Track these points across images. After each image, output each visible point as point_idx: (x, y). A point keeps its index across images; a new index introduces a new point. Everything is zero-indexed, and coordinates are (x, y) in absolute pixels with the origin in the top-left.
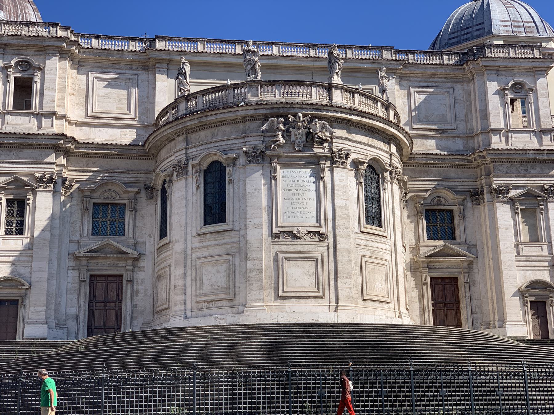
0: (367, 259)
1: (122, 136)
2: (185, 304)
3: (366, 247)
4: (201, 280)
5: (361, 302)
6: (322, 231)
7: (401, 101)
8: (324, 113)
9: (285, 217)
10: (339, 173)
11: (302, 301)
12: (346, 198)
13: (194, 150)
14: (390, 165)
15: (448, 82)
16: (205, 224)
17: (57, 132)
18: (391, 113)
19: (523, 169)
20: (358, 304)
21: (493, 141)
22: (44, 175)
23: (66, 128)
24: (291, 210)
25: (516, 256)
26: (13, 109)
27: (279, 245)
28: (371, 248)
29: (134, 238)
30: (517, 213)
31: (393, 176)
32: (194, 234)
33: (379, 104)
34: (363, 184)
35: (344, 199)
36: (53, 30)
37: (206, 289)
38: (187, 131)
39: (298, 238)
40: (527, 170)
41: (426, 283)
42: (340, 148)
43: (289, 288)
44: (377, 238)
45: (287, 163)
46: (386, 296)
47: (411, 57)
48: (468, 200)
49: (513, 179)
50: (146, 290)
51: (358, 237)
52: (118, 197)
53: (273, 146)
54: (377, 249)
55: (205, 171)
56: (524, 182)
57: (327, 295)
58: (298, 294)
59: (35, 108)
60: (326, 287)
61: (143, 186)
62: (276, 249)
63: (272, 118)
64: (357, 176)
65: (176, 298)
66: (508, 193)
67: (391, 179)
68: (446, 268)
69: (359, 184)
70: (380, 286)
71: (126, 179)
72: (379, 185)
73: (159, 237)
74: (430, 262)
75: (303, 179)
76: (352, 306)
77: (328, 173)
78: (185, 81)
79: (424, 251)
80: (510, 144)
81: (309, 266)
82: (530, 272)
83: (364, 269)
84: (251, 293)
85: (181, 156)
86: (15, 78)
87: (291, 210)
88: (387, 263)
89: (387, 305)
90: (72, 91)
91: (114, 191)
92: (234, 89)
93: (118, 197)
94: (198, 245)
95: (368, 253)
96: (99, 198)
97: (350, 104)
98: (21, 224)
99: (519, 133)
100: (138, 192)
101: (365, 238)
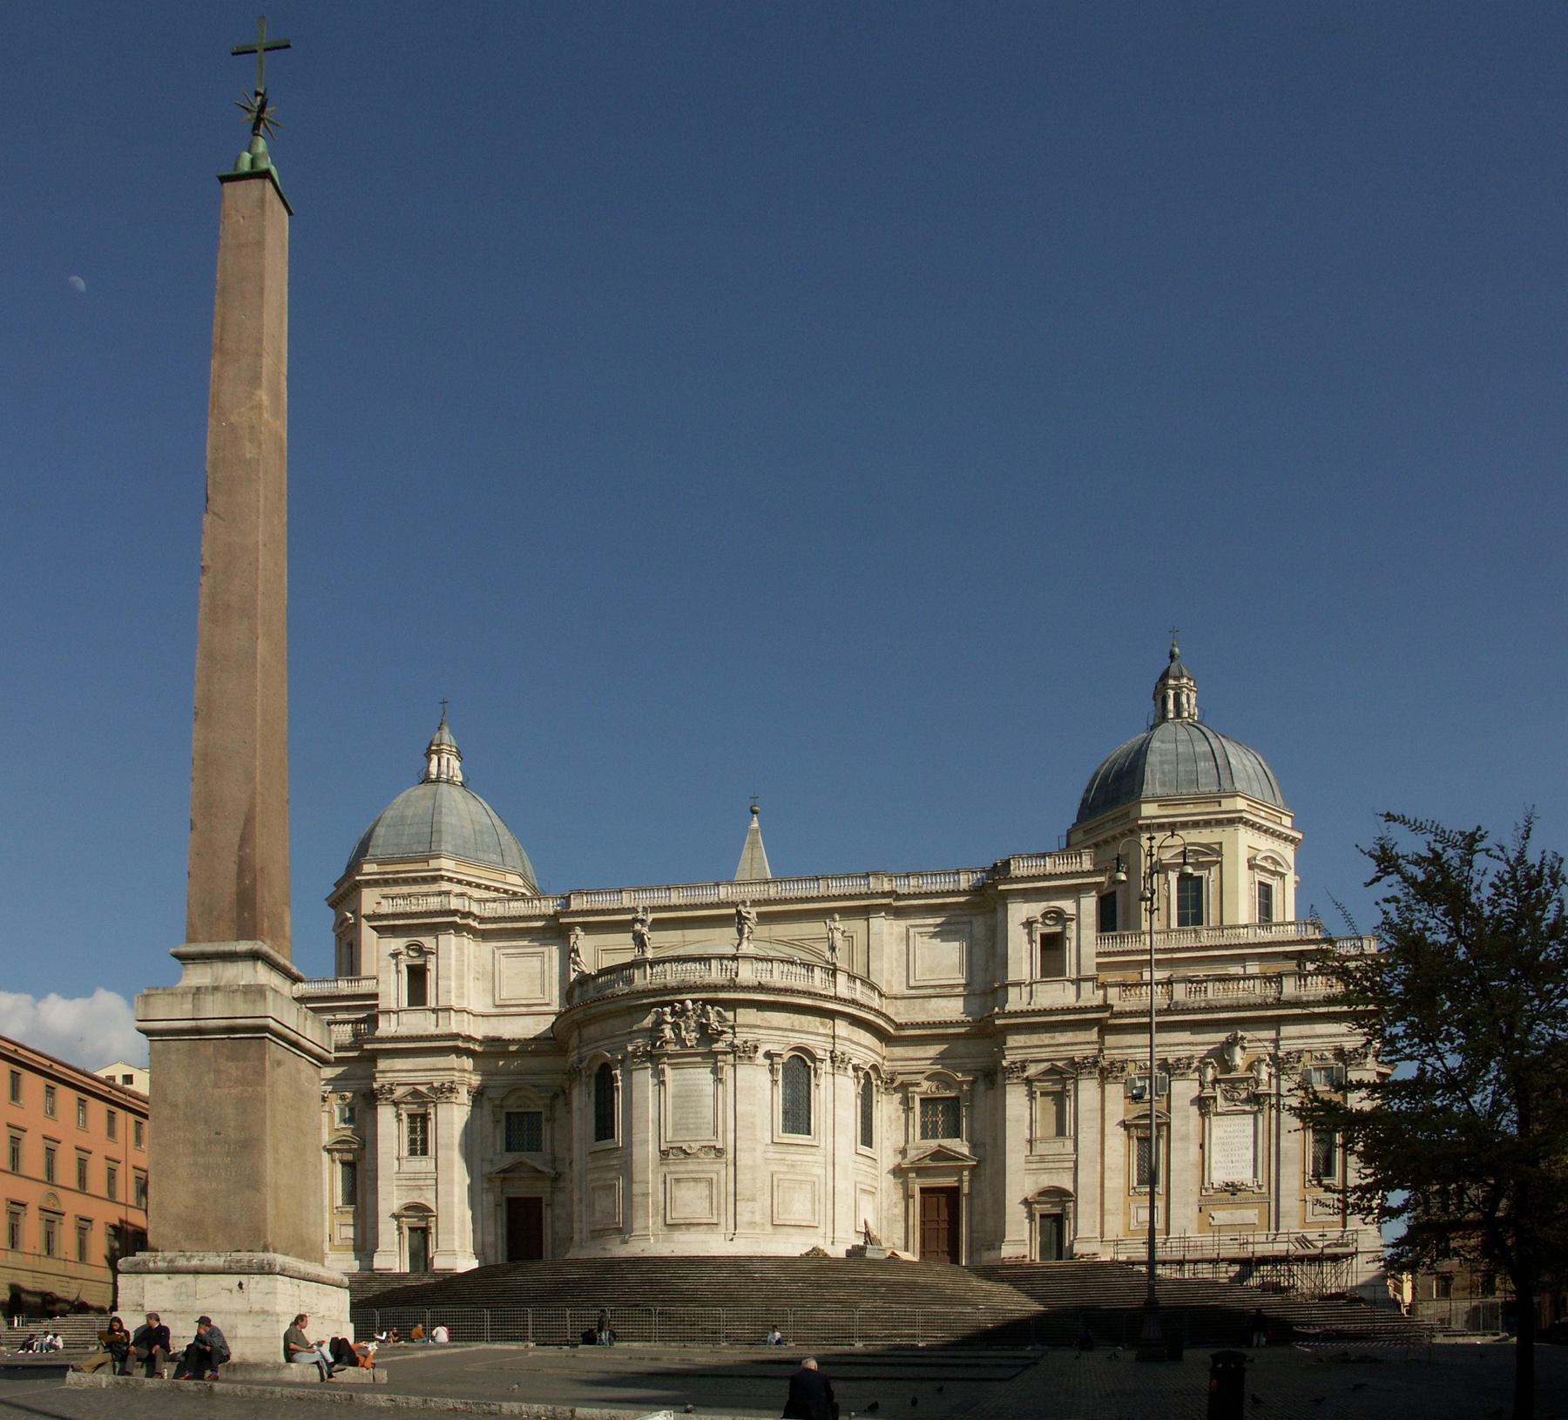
0: (781, 1176)
4: (594, 1204)
5: (769, 1228)
6: (719, 1146)
9: (675, 1130)
10: (744, 1071)
11: (693, 1229)
13: (585, 1049)
14: (832, 1052)
20: (764, 1230)
21: (1009, 999)
22: (443, 1084)
23: (469, 1023)
24: (684, 1121)
26: (409, 1005)
27: (667, 1165)
30: (1035, 1098)
31: (837, 1065)
34: (780, 1083)
37: (598, 1215)
38: (579, 1025)
39: (689, 1154)
42: (744, 1039)
43: (677, 1215)
44: (801, 1149)
45: (678, 1064)
53: (658, 1044)
56: (1047, 1054)
57: (723, 1220)
58: (688, 1221)
60: (723, 1212)
61: (560, 1089)
62: (665, 1168)
66: (1024, 1071)
67: (834, 1069)
69: (774, 1082)
72: (809, 1081)
74: (919, 1168)
75: (698, 1082)
77: (728, 1072)
80: (1032, 1003)
81: (702, 1189)
83: (775, 1188)
84: (638, 1221)
87: (684, 1121)
88: (815, 1179)
89: (812, 1229)
93: (532, 1106)
94: (590, 1165)
95: (784, 1169)
97: (765, 979)
100: (555, 1097)
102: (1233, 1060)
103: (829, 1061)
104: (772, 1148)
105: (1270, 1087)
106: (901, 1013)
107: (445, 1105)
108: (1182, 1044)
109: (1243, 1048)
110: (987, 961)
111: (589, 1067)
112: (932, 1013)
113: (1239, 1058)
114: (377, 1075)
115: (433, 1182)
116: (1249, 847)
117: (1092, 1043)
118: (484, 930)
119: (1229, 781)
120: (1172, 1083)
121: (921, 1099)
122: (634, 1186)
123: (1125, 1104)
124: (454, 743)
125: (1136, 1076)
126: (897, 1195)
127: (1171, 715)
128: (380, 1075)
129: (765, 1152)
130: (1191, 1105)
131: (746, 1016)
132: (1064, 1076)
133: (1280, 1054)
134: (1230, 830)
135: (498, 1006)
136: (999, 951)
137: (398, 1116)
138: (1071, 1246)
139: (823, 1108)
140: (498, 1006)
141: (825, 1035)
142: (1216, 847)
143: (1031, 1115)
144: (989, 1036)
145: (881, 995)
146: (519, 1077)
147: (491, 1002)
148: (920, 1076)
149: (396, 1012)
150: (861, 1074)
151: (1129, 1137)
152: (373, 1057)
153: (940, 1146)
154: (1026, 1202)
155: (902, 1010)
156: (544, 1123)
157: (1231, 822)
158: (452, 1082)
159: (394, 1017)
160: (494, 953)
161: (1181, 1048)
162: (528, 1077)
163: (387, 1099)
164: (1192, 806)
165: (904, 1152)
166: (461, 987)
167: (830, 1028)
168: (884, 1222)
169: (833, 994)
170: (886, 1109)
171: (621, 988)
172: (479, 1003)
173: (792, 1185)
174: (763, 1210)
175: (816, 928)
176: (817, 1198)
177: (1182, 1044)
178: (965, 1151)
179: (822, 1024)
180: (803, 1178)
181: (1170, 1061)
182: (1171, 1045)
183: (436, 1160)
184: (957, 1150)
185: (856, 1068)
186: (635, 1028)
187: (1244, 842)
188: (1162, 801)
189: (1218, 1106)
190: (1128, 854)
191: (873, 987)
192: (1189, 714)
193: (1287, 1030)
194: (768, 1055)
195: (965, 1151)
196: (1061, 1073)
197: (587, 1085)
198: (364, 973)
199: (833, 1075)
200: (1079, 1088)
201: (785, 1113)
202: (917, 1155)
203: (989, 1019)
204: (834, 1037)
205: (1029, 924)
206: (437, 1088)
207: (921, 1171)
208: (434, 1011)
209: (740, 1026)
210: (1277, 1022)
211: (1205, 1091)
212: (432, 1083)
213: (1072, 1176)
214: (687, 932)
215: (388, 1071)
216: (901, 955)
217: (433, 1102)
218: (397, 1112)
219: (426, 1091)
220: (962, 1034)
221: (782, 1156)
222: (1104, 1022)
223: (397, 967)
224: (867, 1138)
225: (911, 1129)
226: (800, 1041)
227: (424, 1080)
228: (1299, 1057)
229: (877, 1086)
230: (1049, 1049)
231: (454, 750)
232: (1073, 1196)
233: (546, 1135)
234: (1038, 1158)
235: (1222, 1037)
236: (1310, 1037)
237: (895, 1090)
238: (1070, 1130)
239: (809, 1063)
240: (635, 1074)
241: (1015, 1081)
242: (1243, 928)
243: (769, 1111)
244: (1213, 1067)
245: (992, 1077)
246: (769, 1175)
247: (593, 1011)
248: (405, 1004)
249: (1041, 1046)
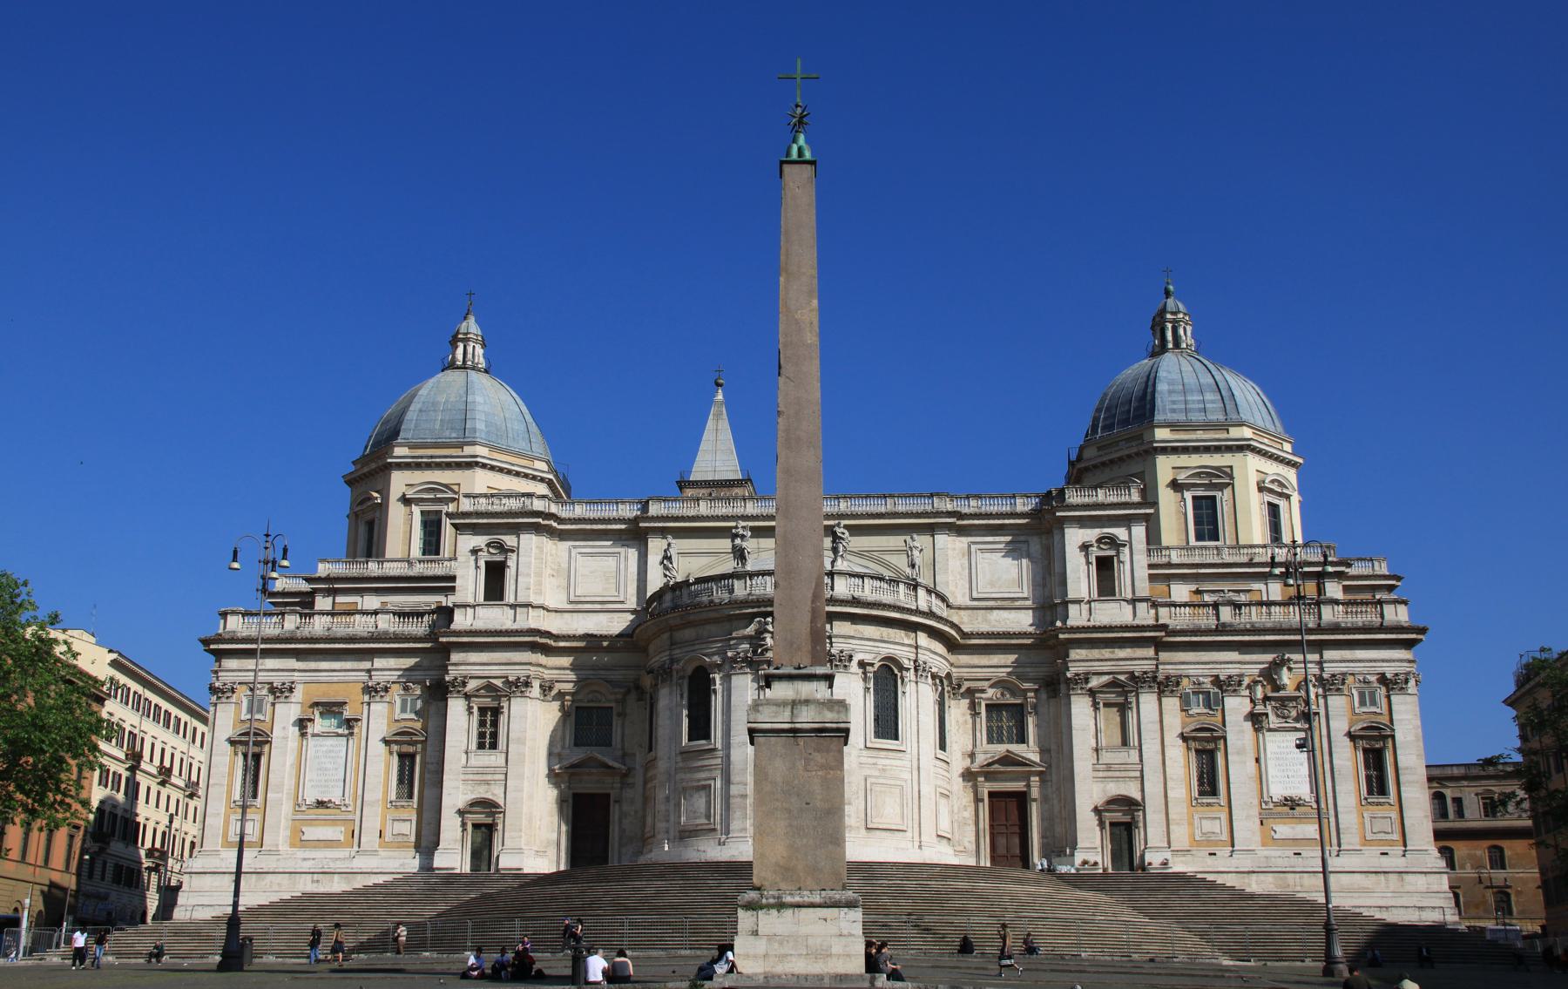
0: (873, 780)
1: (610, 624)
2: (667, 832)
5: (863, 831)
7: (958, 563)
13: (677, 651)
14: (915, 661)
15: (1022, 535)
16: (689, 740)
17: (532, 627)
18: (921, 592)
23: (544, 618)
28: (881, 767)
29: (623, 749)
30: (1098, 709)
31: (920, 673)
32: (678, 752)
33: (902, 586)
34: (872, 690)
36: (528, 501)
41: (982, 800)
44: (890, 753)
46: (901, 823)
47: (973, 503)
48: (1042, 689)
50: (636, 812)
52: (604, 700)
53: (759, 651)
55: (691, 678)
56: (1109, 668)
59: (509, 597)
63: (758, 619)
64: (865, 679)
65: (661, 825)
66: (1087, 682)
70: (892, 811)
71: (612, 677)
73: (647, 750)
74: (988, 772)
78: (670, 566)
79: (981, 759)
80: (1092, 620)
83: (868, 792)
84: (735, 822)
85: (664, 657)
86: (487, 563)
88: (903, 783)
89: (901, 833)
90: (552, 572)
91: (601, 693)
92: (721, 580)
94: (681, 765)
95: (877, 773)
96: (581, 701)
97: (857, 594)
98: (494, 735)
100: (628, 692)
102: (1280, 678)
103: (912, 671)
104: (865, 753)
105: (1318, 707)
106: (969, 622)
107: (519, 699)
108: (1231, 663)
109: (1290, 669)
110: (1044, 578)
111: (683, 669)
112: (996, 624)
113: (1286, 678)
114: (449, 668)
115: (503, 777)
116: (1258, 471)
117: (1150, 659)
118: (562, 530)
119: (1235, 411)
120: (1225, 699)
121: (987, 705)
122: (731, 786)
123: (1182, 718)
124: (480, 333)
125: (1190, 691)
126: (968, 797)
127: (1170, 345)
128: (453, 668)
129: (859, 756)
130: (1245, 721)
131: (841, 628)
132: (1126, 689)
133: (1325, 676)
134: (1239, 455)
135: (571, 602)
136: (1057, 569)
137: (470, 709)
138: (1142, 856)
139: (908, 716)
140: (571, 602)
142: (1228, 470)
143: (1096, 725)
144: (1051, 648)
145: (948, 606)
146: (592, 672)
147: (565, 599)
148: (986, 684)
149: (474, 607)
150: (938, 681)
151: (1188, 749)
152: (447, 649)
153: (1008, 751)
154: (1096, 810)
155: (966, 619)
156: (615, 718)
157: (1240, 449)
158: (528, 677)
159: (470, 611)
160: (570, 552)
161: (1230, 666)
162: (602, 672)
163: (459, 692)
164: (1201, 432)
165: (972, 756)
166: (540, 584)
168: (956, 825)
169: (914, 608)
170: (958, 711)
171: (720, 595)
172: (555, 599)
173: (883, 789)
175: (896, 541)
177: (1231, 663)
178: (1036, 758)
179: (906, 635)
180: (893, 782)
181: (1222, 678)
182: (1221, 663)
183: (507, 753)
184: (1024, 755)
185: (934, 677)
186: (734, 635)
187: (1250, 469)
188: (1173, 426)
189: (1270, 722)
190: (1143, 472)
191: (943, 598)
192: (1187, 345)
193: (1329, 654)
194: (862, 664)
195: (1036, 758)
196: (1123, 686)
197: (681, 686)
198: (388, 555)
199: (917, 683)
200: (1140, 700)
201: (877, 720)
202: (986, 760)
203: (1052, 633)
204: (917, 647)
205: (1085, 547)
206: (512, 682)
207: (989, 776)
208: (513, 606)
209: (836, 636)
210: (1319, 646)
211: (1257, 707)
212: (507, 677)
213: (1139, 785)
214: (761, 540)
215: (461, 664)
216: (963, 569)
217: (506, 696)
218: (469, 703)
219: (501, 685)
220: (1027, 645)
221: (874, 761)
222: (1160, 639)
223: (476, 563)
224: (943, 747)
225: (978, 734)
226: (887, 651)
227: (499, 673)
228: (1344, 679)
229: (948, 692)
230: (1109, 663)
231: (480, 338)
232: (1140, 805)
233: (616, 731)
234: (1104, 766)
235: (1269, 657)
236: (1352, 661)
237: (963, 696)
238: (1133, 739)
239: (896, 671)
240: (734, 678)
241: (1079, 692)
242: (1262, 547)
243: (862, 717)
244: (1263, 686)
245: (1056, 686)
246: (863, 778)
247: (692, 617)
248: (481, 598)
249: (1102, 660)
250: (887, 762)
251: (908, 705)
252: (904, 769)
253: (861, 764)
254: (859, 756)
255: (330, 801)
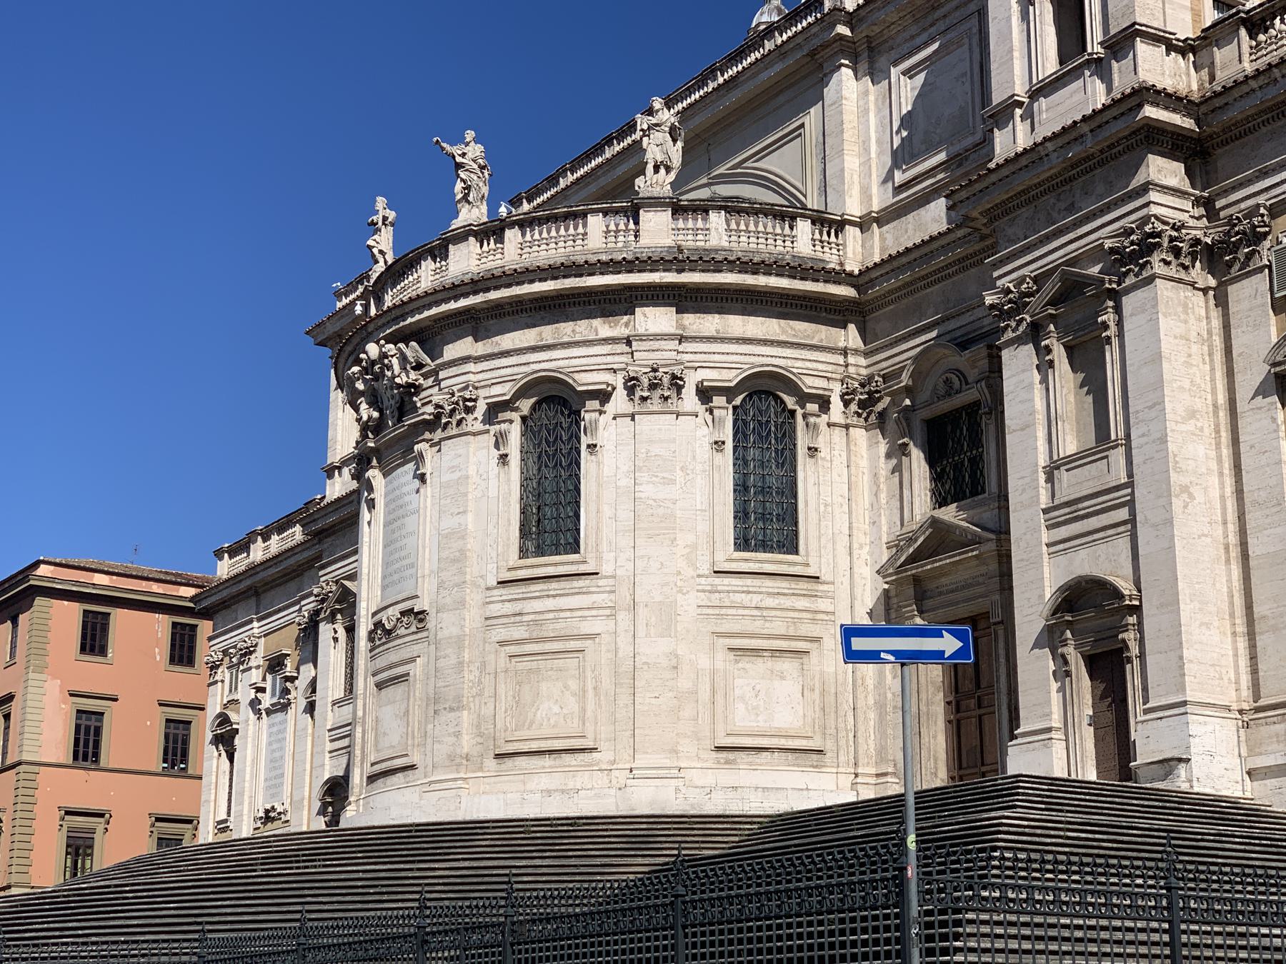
3: (513, 619)
5: (491, 763)
8: (410, 320)
12: (461, 510)
19: (1062, 205)
20: (481, 769)
25: (1045, 511)
28: (532, 617)
30: (1051, 364)
35: (459, 513)
40: (1071, 209)
44: (554, 586)
49: (1037, 253)
51: (492, 599)
54: (551, 615)
68: (963, 587)
70: (556, 709)
76: (455, 780)
82: (1083, 553)
89: (580, 756)
99: (1057, 90)
101: (510, 597)
103: (620, 395)
141: (606, 341)
167: (627, 325)
174: (478, 726)
176: (590, 685)
185: (705, 394)
221: (517, 607)
250: (550, 604)
251: (607, 471)
252: (594, 612)
253: (486, 619)
254: (488, 603)
255: (273, 808)
